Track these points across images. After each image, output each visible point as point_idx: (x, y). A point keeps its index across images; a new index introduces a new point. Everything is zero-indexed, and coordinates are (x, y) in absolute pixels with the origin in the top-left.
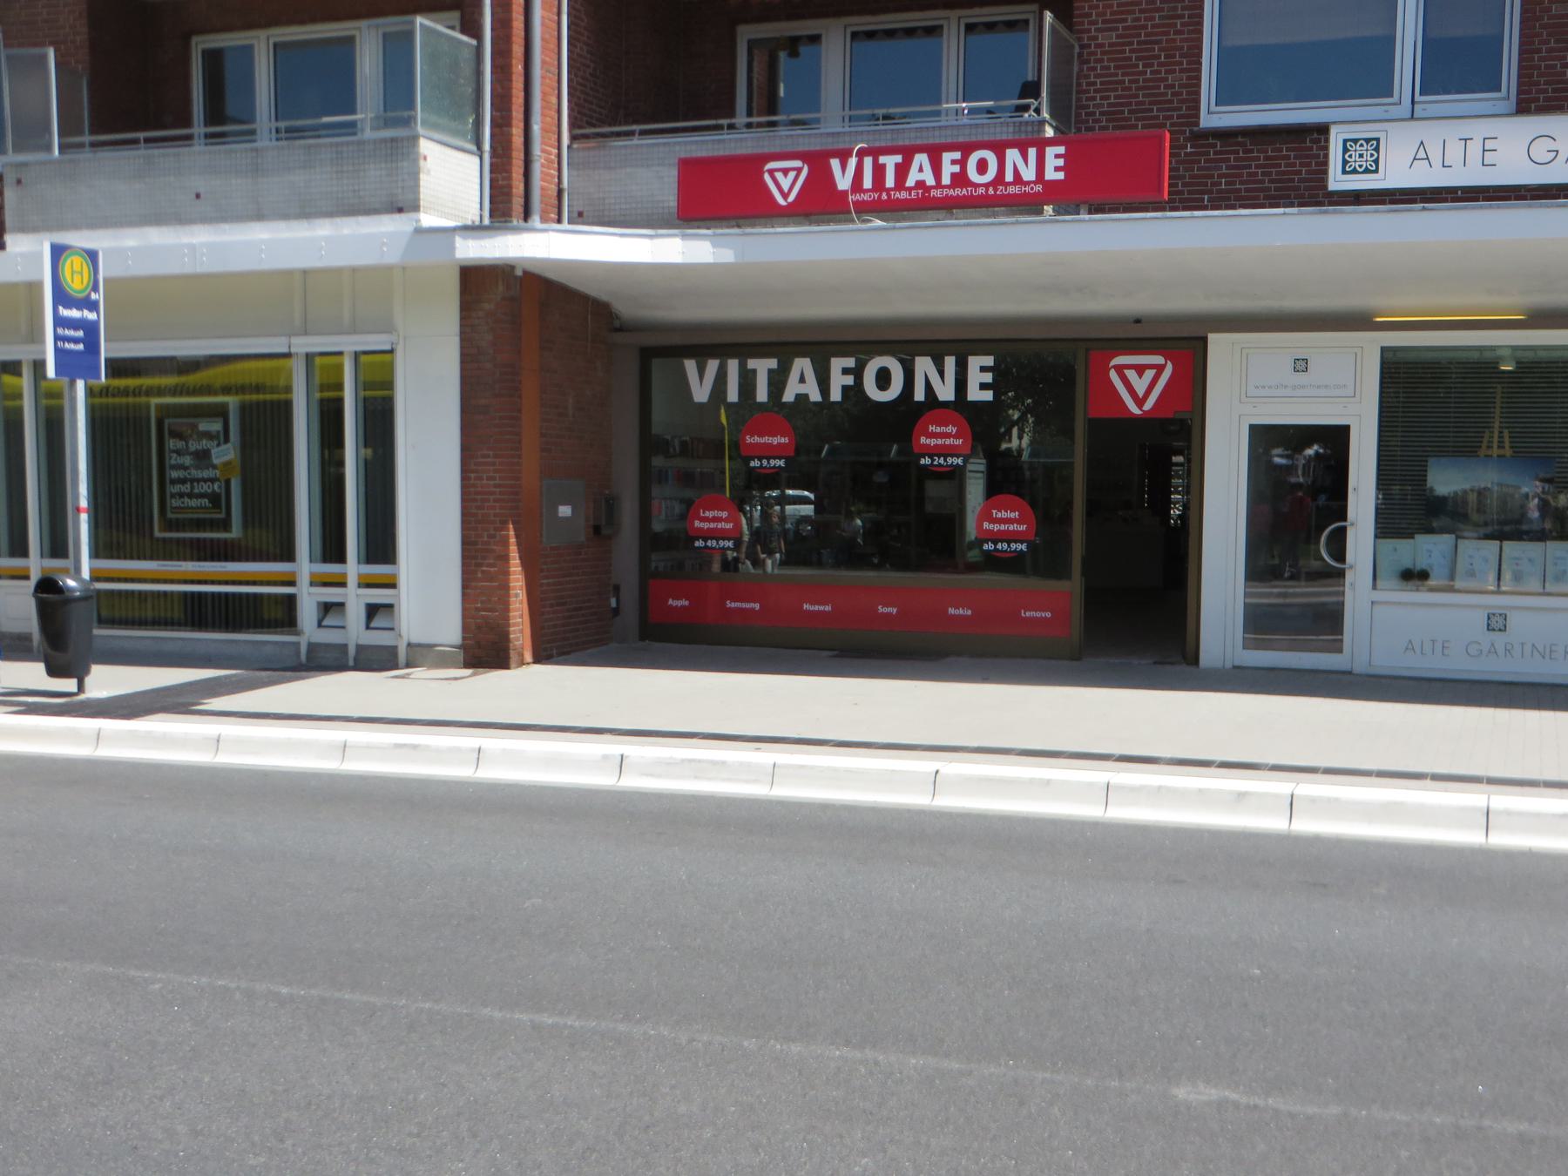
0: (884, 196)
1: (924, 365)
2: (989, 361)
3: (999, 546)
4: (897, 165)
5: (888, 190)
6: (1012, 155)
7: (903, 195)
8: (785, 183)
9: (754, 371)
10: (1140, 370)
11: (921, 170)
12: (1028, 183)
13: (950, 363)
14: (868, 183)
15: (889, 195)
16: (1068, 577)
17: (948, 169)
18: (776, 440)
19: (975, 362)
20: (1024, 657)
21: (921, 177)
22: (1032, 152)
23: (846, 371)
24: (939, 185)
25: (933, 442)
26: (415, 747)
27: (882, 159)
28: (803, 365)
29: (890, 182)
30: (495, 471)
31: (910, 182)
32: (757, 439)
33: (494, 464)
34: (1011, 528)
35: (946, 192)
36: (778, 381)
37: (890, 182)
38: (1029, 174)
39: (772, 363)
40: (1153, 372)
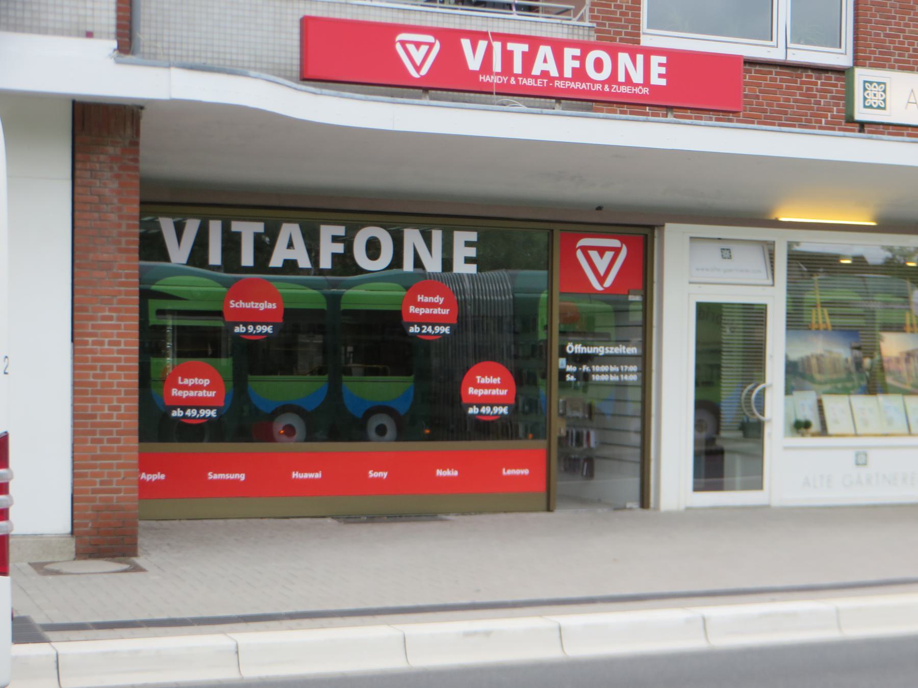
0: (513, 81)
1: (412, 237)
2: (473, 236)
4: (524, 53)
5: (516, 76)
6: (624, 58)
7: (530, 82)
8: (418, 56)
9: (238, 235)
10: (602, 251)
11: (545, 61)
12: (637, 85)
13: (437, 236)
14: (497, 66)
15: (517, 80)
17: (570, 64)
18: (263, 306)
19: (460, 237)
20: (505, 512)
21: (545, 67)
22: (640, 58)
23: (335, 239)
24: (561, 77)
25: (421, 311)
26: (487, 634)
27: (510, 46)
28: (290, 231)
29: (518, 68)
30: (119, 335)
31: (536, 71)
32: (242, 304)
33: (118, 327)
34: (495, 392)
35: (568, 84)
37: (518, 68)
38: (638, 77)
39: (259, 227)
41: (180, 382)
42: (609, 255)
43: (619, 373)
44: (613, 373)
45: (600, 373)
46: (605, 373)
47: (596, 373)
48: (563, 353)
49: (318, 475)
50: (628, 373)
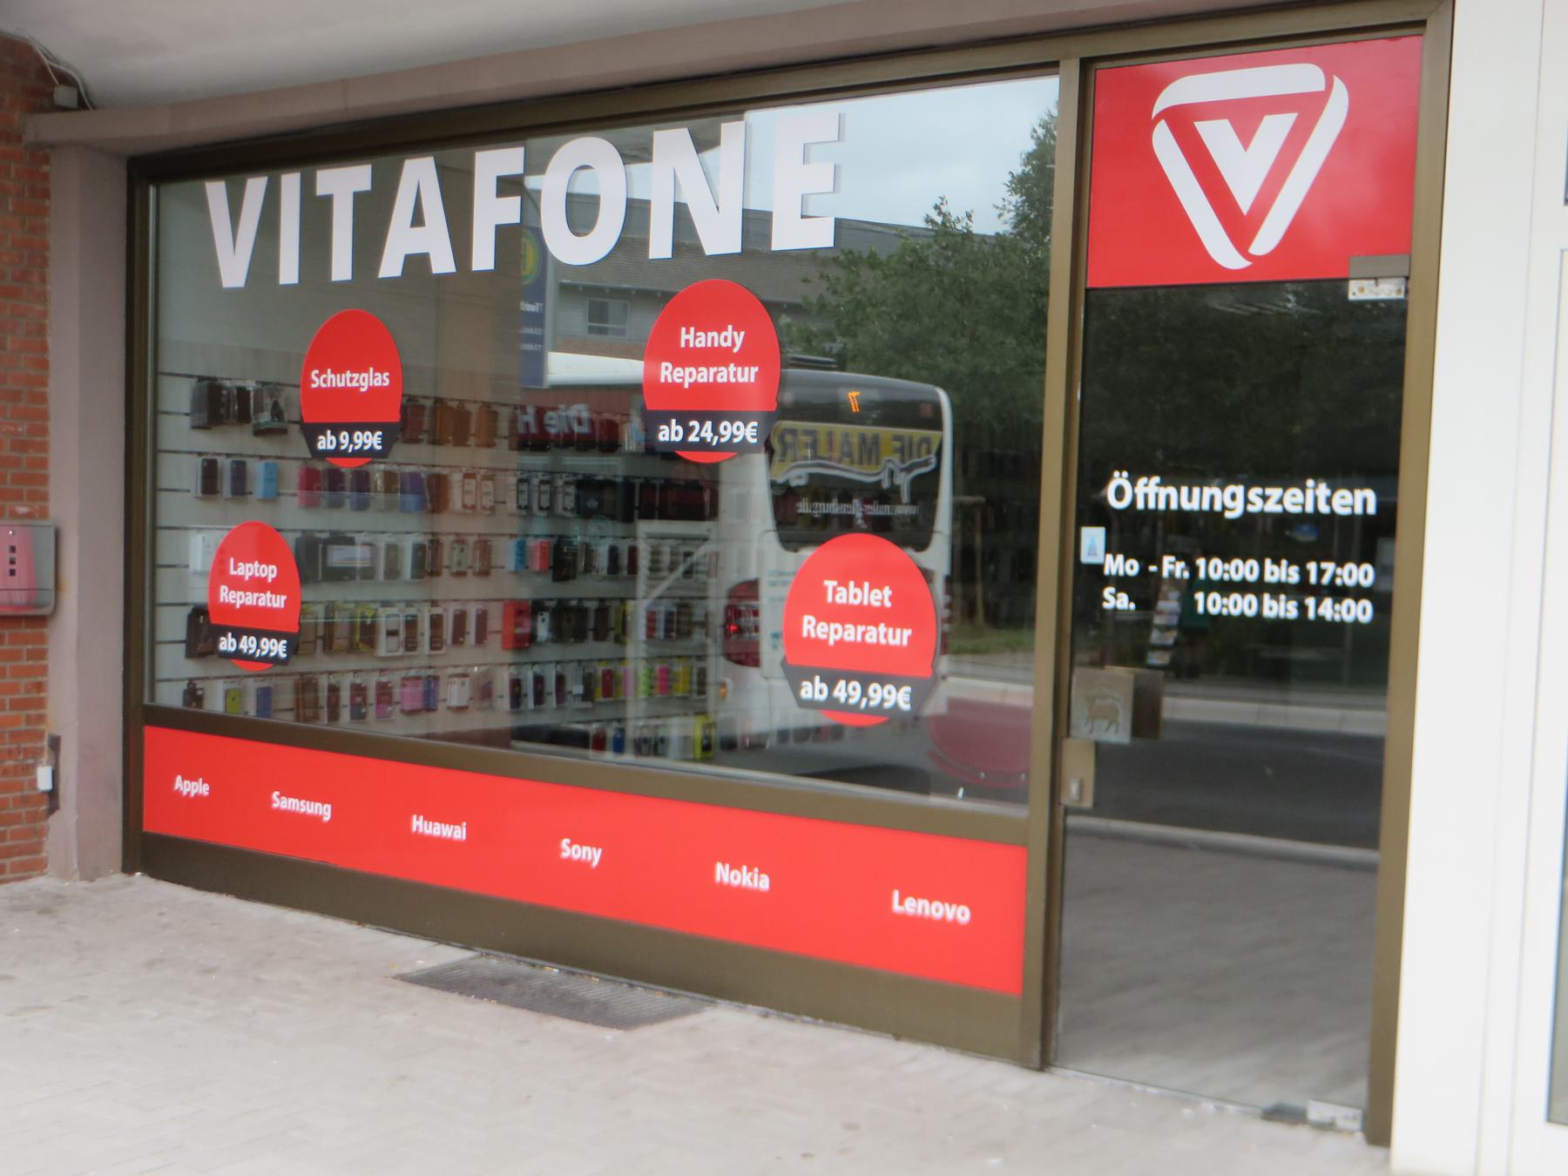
3: (841, 691)
9: (328, 201)
10: (1245, 115)
16: (1017, 795)
34: (876, 634)
36: (372, 216)
40: (1288, 119)
41: (232, 572)
42: (1275, 128)
43: (1301, 590)
44: (1278, 589)
45: (1226, 587)
46: (1243, 587)
47: (1210, 586)
48: (1096, 513)
49: (459, 833)
50: (1339, 593)
